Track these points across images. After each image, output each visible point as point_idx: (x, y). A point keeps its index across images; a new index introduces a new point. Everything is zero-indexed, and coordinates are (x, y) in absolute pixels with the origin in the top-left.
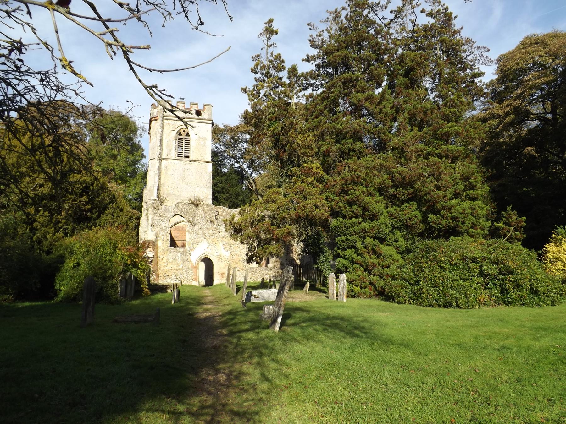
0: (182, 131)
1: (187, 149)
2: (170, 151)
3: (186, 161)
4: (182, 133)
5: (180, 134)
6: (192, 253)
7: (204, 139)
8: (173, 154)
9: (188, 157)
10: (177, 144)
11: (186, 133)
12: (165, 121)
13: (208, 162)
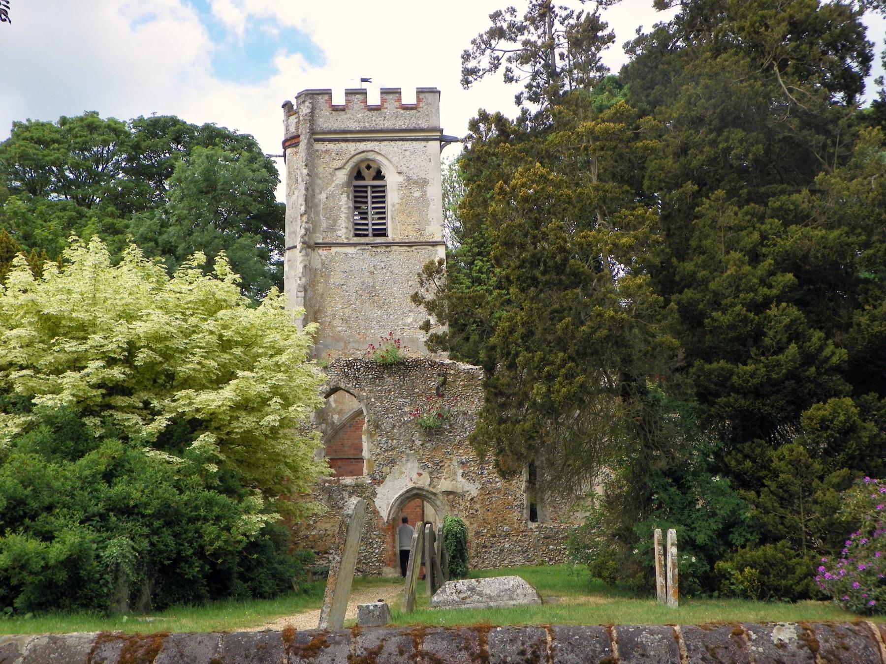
1: (382, 213)
2: (335, 221)
3: (375, 246)
4: (365, 173)
6: (379, 490)
7: (423, 183)
10: (351, 204)
11: (373, 172)
12: (319, 146)
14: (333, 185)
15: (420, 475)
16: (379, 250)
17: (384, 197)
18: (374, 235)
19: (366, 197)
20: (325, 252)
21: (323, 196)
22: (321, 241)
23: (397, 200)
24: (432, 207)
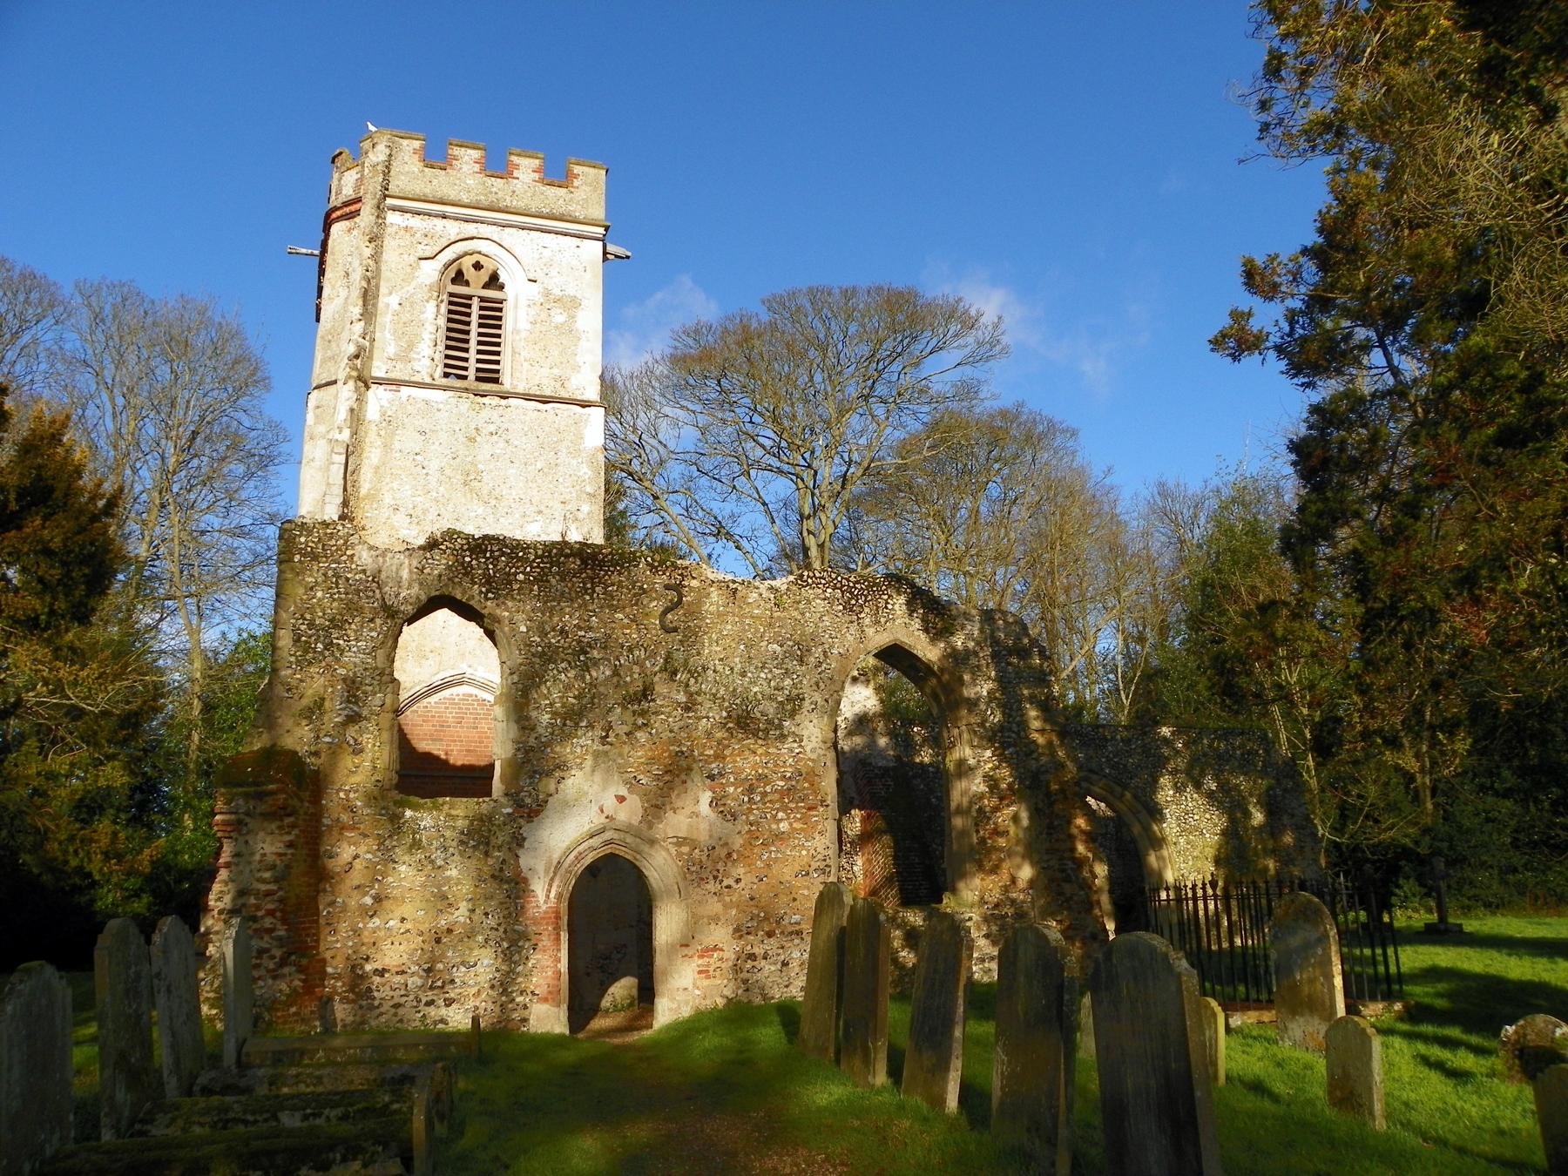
0: (467, 263)
2: (411, 346)
4: (470, 273)
5: (459, 278)
7: (571, 304)
8: (427, 356)
9: (496, 381)
10: (442, 322)
11: (484, 276)
12: (392, 218)
13: (585, 405)
14: (414, 284)
15: (621, 799)
16: (486, 400)
17: (500, 318)
18: (478, 379)
19: (469, 315)
20: (390, 395)
21: (393, 301)
22: (382, 375)
23: (524, 325)
24: (583, 343)
